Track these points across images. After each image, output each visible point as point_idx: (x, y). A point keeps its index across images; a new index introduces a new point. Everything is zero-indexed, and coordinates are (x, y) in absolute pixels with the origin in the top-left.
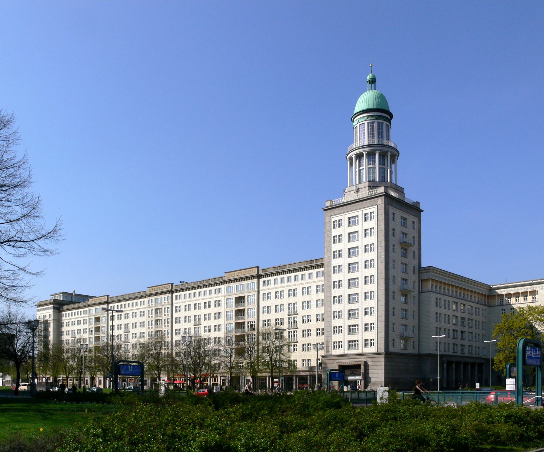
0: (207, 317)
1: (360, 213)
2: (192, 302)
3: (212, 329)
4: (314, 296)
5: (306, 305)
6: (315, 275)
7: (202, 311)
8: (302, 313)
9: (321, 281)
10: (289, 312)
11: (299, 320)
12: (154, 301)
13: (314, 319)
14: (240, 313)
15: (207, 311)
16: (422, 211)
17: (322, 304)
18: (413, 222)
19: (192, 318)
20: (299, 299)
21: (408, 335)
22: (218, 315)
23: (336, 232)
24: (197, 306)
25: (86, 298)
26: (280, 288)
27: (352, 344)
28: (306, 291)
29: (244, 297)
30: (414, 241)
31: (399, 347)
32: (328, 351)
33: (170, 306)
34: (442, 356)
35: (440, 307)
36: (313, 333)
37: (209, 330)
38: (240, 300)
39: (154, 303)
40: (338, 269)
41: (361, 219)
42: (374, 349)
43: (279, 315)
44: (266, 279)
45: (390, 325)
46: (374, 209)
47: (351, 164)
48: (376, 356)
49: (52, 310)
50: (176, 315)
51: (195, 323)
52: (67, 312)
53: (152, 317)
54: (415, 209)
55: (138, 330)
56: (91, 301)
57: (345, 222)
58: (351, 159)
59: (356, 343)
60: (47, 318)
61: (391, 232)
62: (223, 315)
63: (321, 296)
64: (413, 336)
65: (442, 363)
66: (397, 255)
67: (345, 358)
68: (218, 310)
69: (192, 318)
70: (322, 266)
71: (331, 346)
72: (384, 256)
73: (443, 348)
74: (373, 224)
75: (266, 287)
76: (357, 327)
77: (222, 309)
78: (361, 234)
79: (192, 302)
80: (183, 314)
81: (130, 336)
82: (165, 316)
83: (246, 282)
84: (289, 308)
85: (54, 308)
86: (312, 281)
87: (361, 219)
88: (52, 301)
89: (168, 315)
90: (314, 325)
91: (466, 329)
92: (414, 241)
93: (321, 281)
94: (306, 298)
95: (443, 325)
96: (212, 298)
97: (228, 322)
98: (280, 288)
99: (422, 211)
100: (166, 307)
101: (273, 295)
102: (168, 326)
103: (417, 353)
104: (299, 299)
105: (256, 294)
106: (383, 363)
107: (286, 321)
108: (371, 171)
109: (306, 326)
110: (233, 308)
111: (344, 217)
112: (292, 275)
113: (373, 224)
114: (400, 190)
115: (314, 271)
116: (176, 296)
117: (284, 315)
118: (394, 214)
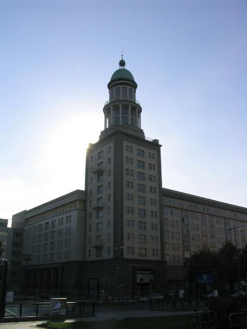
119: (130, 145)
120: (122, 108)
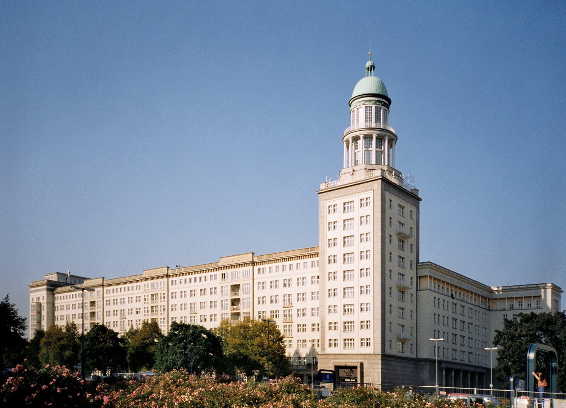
0: (202, 305)
2: (188, 287)
3: (208, 318)
4: (309, 288)
5: (301, 297)
6: (309, 264)
7: (198, 299)
8: (297, 305)
9: (316, 271)
10: (284, 304)
11: (294, 312)
12: (150, 285)
14: (235, 302)
15: (203, 299)
16: (420, 200)
17: (318, 297)
18: (412, 212)
19: (188, 306)
20: (294, 290)
21: (405, 337)
22: (213, 304)
23: (331, 218)
24: (193, 293)
25: (82, 279)
26: (275, 277)
28: (301, 281)
29: (239, 285)
30: (411, 232)
31: (395, 349)
33: (166, 292)
34: (440, 362)
35: (439, 308)
36: (309, 328)
37: (205, 320)
38: (235, 288)
39: (150, 288)
40: (332, 260)
41: (357, 204)
43: (274, 307)
45: (386, 324)
47: (348, 147)
49: (45, 292)
50: (172, 302)
51: (191, 312)
52: (62, 295)
53: (148, 303)
54: (413, 197)
55: (134, 317)
56: (86, 284)
57: (340, 208)
58: (348, 141)
59: (352, 342)
60: (41, 301)
61: (387, 220)
62: (219, 304)
63: (316, 288)
64: (410, 338)
65: (440, 370)
66: (393, 247)
68: (213, 298)
69: (188, 306)
72: (380, 247)
73: (441, 354)
74: (368, 210)
75: (261, 275)
76: (352, 324)
77: (217, 297)
78: (357, 221)
79: (188, 287)
80: (179, 301)
81: (126, 323)
82: (161, 303)
83: (241, 269)
84: (284, 300)
85: (48, 290)
88: (46, 281)
89: (164, 301)
90: (309, 320)
91: (466, 334)
92: (411, 232)
94: (301, 289)
95: (442, 328)
96: (208, 285)
97: (224, 312)
98: (275, 277)
99: (420, 200)
100: (162, 292)
101: (268, 285)
102: (164, 314)
103: (415, 357)
104: (294, 290)
105: (251, 282)
106: (380, 366)
107: (281, 314)
108: (368, 153)
109: (301, 320)
110: (229, 297)
112: (287, 263)
114: (398, 175)
115: (309, 260)
116: (172, 281)
117: (279, 307)
118: (391, 201)
119: (392, 198)
120: (377, 138)
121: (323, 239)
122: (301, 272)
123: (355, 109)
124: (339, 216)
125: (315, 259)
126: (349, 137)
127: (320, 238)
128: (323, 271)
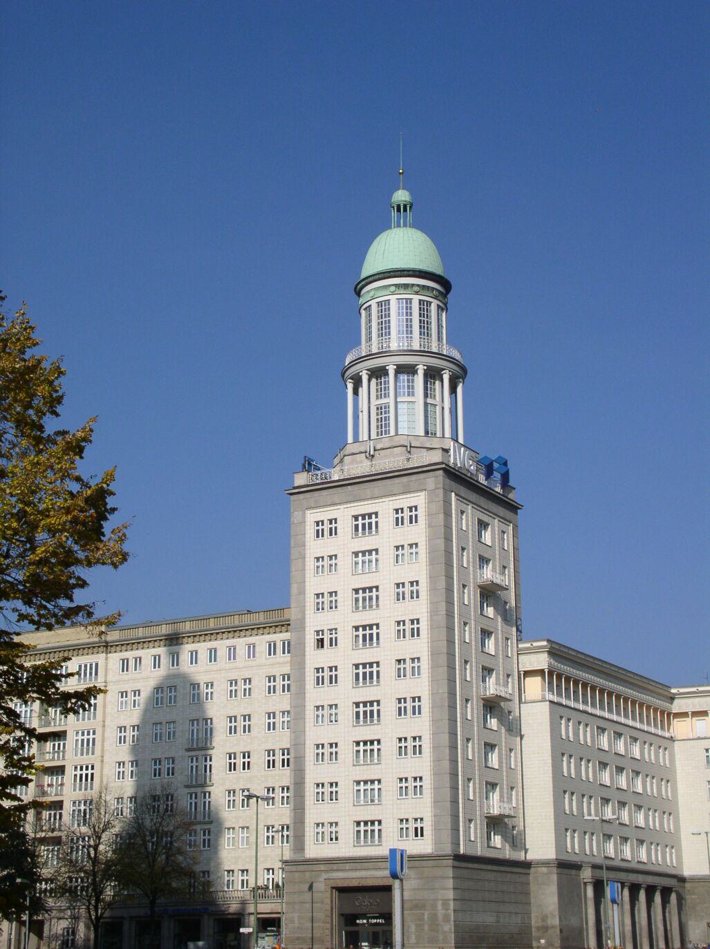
1: (385, 508)
13: (258, 760)
27: (368, 828)
32: (299, 845)
42: (424, 846)
44: (130, 655)
46: (420, 499)
48: (431, 863)
57: (345, 525)
63: (282, 702)
67: (347, 866)
70: (284, 625)
71: (310, 832)
76: (376, 786)
86: (254, 663)
87: (386, 520)
93: (282, 664)
94: (239, 707)
111: (344, 514)
113: (418, 533)
121: (302, 592)
122: (241, 667)
123: (373, 303)
124: (345, 543)
125: (279, 637)
126: (363, 370)
127: (294, 589)
128: (299, 664)
